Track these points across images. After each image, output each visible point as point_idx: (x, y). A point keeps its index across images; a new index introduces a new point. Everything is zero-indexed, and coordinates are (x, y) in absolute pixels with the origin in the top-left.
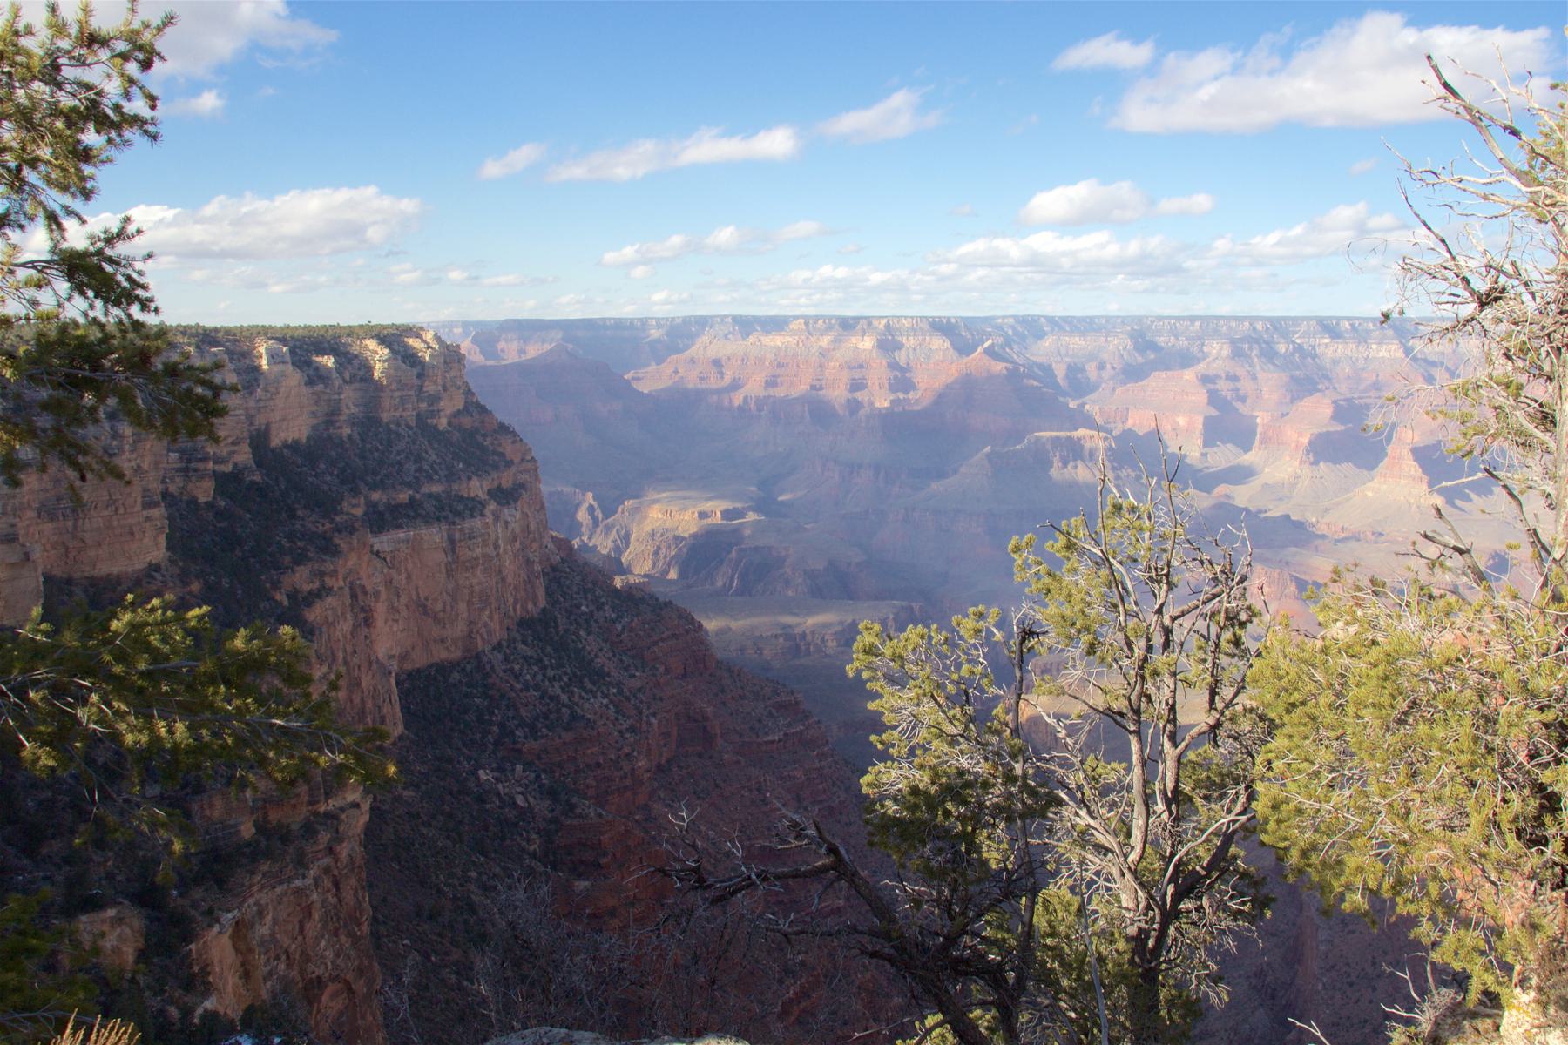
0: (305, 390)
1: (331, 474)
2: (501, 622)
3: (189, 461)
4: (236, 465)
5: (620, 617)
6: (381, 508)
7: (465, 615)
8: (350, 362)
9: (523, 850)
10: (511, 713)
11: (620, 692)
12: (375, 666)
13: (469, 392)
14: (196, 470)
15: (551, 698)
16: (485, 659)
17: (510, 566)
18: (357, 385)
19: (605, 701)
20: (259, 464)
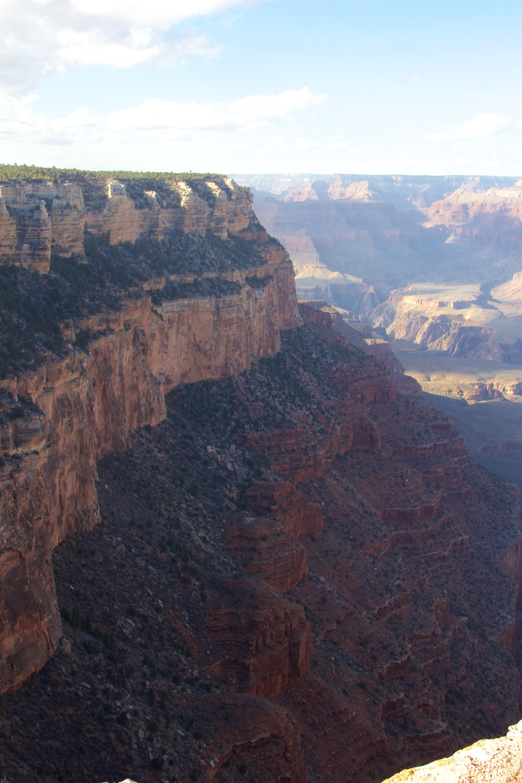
0: (137, 213)
1: (146, 263)
2: (247, 358)
3: (35, 250)
4: (73, 254)
5: (335, 363)
6: (175, 285)
7: (223, 353)
8: (168, 196)
9: (226, 496)
10: (244, 414)
11: (319, 408)
12: (149, 378)
13: (254, 218)
14: (39, 255)
15: (271, 408)
16: (234, 380)
17: (257, 325)
18: (171, 210)
19: (307, 413)
20: (88, 254)
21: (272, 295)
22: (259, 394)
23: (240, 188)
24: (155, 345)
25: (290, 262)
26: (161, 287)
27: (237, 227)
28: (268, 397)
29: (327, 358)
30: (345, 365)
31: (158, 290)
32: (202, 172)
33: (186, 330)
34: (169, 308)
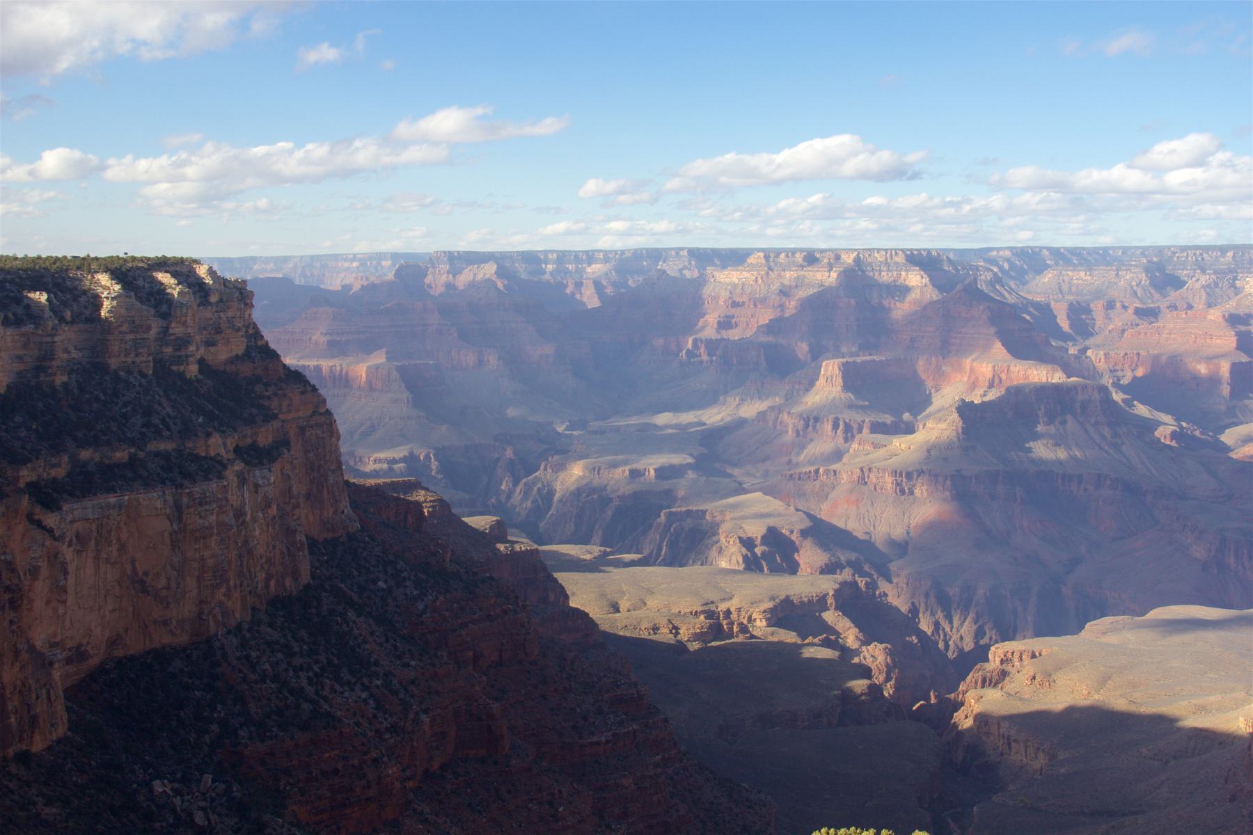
8: (75, 299)
13: (257, 335)
16: (217, 644)
17: (260, 536)
19: (364, 695)
21: (289, 478)
22: (267, 666)
23: (225, 282)
24: (41, 588)
25: (328, 413)
26: (60, 473)
27: (221, 354)
28: (286, 670)
29: (405, 587)
30: (441, 598)
31: (55, 479)
32: (152, 255)
33: (115, 553)
34: (76, 514)
